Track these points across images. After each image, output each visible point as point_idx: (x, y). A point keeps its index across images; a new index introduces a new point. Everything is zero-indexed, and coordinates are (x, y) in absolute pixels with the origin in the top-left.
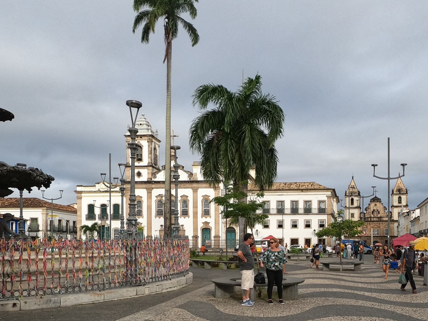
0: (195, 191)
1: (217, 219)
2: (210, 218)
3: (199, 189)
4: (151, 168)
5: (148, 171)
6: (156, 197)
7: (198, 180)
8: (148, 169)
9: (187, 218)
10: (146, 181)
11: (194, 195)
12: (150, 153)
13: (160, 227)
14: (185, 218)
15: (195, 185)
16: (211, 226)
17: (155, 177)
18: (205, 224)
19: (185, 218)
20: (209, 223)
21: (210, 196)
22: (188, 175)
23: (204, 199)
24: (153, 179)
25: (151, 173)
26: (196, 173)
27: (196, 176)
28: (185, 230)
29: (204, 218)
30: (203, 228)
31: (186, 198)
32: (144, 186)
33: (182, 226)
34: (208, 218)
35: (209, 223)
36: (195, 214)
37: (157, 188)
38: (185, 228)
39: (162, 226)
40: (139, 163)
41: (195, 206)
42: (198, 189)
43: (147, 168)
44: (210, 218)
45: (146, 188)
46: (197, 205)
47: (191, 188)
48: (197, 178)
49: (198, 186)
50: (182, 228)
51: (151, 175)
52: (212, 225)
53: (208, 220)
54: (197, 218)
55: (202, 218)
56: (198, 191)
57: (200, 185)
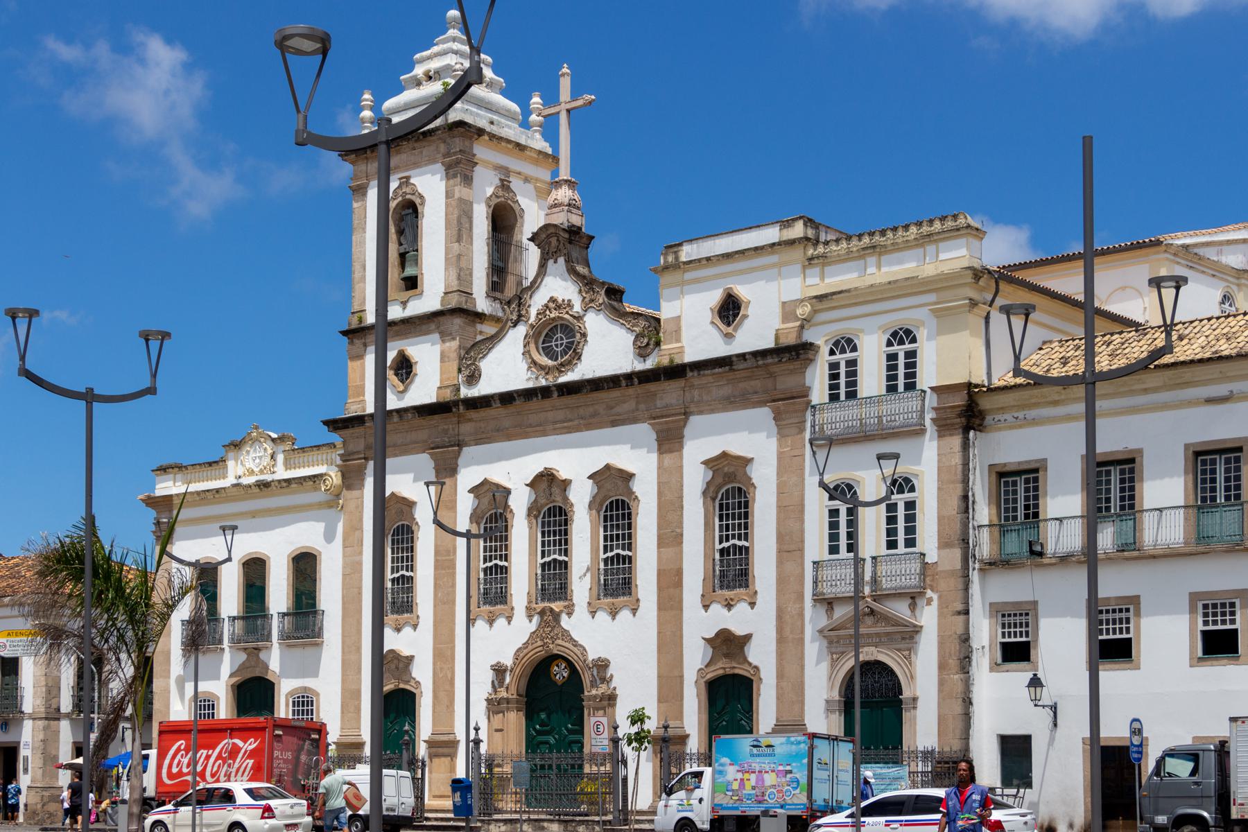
1: (792, 608)
2: (752, 605)
4: (458, 321)
7: (689, 358)
9: (625, 614)
10: (434, 400)
12: (455, 233)
14: (614, 618)
17: (473, 378)
19: (614, 619)
24: (466, 392)
25: (454, 355)
26: (679, 317)
27: (678, 340)
29: (716, 608)
30: (709, 676)
32: (423, 435)
33: (602, 665)
34: (742, 607)
35: (748, 637)
36: (670, 581)
40: (404, 304)
41: (670, 537)
42: (685, 421)
45: (432, 447)
48: (681, 351)
53: (720, 618)
54: (680, 608)
55: (706, 607)
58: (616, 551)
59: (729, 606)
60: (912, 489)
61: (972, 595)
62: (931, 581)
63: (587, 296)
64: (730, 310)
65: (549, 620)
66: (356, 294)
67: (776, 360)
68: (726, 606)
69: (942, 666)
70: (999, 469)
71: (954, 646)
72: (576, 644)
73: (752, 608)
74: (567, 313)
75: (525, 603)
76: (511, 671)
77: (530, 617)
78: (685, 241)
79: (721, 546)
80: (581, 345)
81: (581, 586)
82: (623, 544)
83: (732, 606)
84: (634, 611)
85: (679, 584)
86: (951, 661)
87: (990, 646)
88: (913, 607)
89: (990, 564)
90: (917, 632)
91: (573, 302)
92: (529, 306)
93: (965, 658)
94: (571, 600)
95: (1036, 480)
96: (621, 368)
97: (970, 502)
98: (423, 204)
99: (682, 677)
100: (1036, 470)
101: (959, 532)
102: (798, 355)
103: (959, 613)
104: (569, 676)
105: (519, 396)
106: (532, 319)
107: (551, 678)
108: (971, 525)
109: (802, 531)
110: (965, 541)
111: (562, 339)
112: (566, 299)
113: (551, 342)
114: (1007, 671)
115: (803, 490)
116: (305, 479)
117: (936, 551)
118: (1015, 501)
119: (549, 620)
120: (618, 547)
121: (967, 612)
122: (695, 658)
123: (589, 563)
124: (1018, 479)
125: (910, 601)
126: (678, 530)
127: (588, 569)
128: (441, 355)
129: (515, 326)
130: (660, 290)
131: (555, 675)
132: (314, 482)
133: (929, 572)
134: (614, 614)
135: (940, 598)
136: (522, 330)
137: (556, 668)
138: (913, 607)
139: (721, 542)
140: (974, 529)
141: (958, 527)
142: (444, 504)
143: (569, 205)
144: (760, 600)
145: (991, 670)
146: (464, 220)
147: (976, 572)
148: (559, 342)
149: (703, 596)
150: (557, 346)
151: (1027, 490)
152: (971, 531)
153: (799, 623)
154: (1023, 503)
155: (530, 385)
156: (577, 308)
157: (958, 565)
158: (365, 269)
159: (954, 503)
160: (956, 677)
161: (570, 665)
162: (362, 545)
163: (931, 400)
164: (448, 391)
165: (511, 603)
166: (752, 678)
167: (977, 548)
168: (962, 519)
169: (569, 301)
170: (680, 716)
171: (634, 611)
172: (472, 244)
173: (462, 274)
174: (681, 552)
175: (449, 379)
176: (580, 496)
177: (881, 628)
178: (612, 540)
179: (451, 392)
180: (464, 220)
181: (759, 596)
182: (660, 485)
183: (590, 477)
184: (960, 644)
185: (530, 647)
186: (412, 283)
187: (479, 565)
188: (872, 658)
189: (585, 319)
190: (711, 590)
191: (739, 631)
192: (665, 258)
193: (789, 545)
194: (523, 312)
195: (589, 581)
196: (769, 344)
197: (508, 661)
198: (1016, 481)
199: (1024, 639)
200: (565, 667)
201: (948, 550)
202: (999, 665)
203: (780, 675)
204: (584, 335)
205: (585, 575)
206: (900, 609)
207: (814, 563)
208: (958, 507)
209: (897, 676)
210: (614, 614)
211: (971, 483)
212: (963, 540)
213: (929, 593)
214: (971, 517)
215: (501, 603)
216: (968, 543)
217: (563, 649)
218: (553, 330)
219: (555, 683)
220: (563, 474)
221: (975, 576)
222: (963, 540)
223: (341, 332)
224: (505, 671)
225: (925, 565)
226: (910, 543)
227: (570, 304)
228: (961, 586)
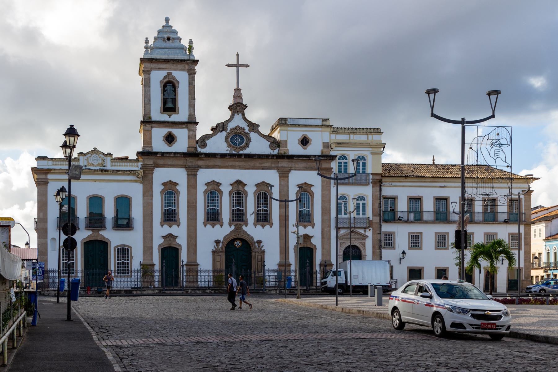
0: (284, 175)
1: (326, 229)
2: (313, 227)
3: (292, 171)
5: (189, 132)
6: (207, 184)
7: (291, 153)
8: (189, 130)
9: (267, 227)
11: (282, 183)
13: (215, 244)
14: (263, 228)
15: (284, 164)
16: (314, 244)
17: (204, 146)
19: (263, 228)
20: (312, 237)
21: (312, 185)
24: (200, 150)
28: (264, 252)
31: (266, 189)
32: (181, 162)
33: (259, 242)
34: (309, 228)
35: (312, 237)
36: (284, 219)
37: (207, 167)
38: (266, 247)
39: (217, 242)
43: (187, 127)
44: (313, 227)
47: (274, 169)
48: (288, 150)
49: (290, 166)
50: (259, 246)
51: (195, 142)
52: (317, 242)
56: (290, 175)
57: (293, 164)
58: (262, 208)
59: (305, 227)
60: (364, 200)
63: (251, 127)
64: (305, 142)
65: (238, 229)
67: (325, 159)
72: (248, 235)
73: (313, 228)
74: (243, 132)
75: (228, 221)
76: (222, 243)
79: (300, 210)
80: (248, 142)
81: (251, 218)
91: (245, 128)
94: (247, 221)
96: (264, 152)
102: (333, 158)
104: (242, 245)
106: (228, 131)
111: (238, 139)
112: (242, 127)
115: (330, 196)
116: (127, 171)
119: (238, 229)
120: (263, 207)
122: (293, 241)
125: (364, 230)
127: (253, 213)
129: (221, 132)
132: (131, 172)
134: (263, 227)
136: (224, 134)
139: (300, 208)
153: (329, 234)
155: (228, 152)
156: (247, 130)
157: (379, 221)
161: (242, 240)
162: (152, 196)
164: (193, 149)
176: (251, 190)
177: (356, 236)
178: (260, 204)
179: (194, 150)
182: (280, 189)
183: (256, 185)
188: (354, 244)
191: (310, 235)
192: (281, 122)
193: (326, 211)
194: (225, 128)
196: (319, 153)
197: (222, 240)
205: (252, 214)
210: (263, 227)
218: (235, 136)
219: (236, 247)
227: (244, 129)
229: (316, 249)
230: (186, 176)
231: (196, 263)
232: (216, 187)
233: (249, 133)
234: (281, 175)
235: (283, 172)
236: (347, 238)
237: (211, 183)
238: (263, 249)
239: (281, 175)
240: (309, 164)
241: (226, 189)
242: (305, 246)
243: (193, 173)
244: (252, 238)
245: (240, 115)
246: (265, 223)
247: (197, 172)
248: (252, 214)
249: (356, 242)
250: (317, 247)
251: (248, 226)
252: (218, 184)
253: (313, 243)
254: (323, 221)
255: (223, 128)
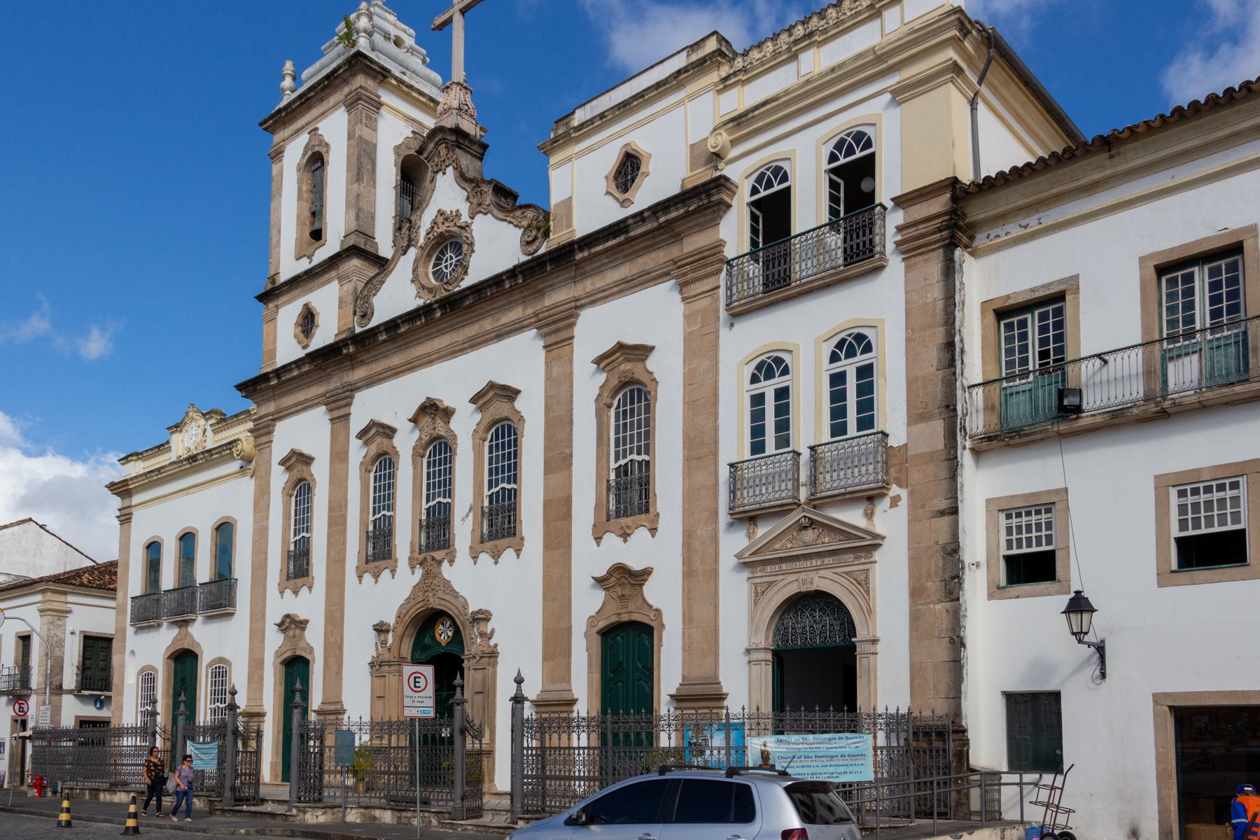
1: (702, 532)
2: (653, 531)
11: (555, 372)
12: (355, 172)
16: (655, 606)
17: (366, 316)
18: (618, 589)
20: (646, 573)
22: (519, 232)
23: (615, 382)
26: (570, 199)
29: (611, 539)
30: (602, 625)
33: (482, 617)
34: (641, 534)
35: (646, 573)
39: (381, 629)
40: (310, 257)
46: (571, 446)
51: (352, 312)
54: (569, 546)
55: (598, 539)
59: (625, 536)
61: (962, 485)
62: (897, 472)
66: (273, 260)
68: (621, 536)
69: (916, 593)
70: (997, 305)
71: (936, 562)
72: (456, 595)
77: (413, 568)
78: (578, 107)
81: (463, 530)
82: (509, 477)
83: (629, 535)
84: (518, 551)
85: (567, 516)
86: (929, 584)
87: (988, 561)
88: (869, 515)
89: (990, 439)
90: (877, 546)
91: (461, 212)
92: (419, 227)
93: (953, 578)
95: (1059, 312)
97: (958, 350)
98: (328, 152)
99: (569, 629)
100: (1060, 297)
101: (940, 396)
103: (942, 513)
104: (454, 634)
105: (403, 322)
107: (435, 638)
108: (958, 383)
109: (716, 429)
110: (950, 407)
113: (441, 264)
114: (1018, 597)
117: (905, 428)
118: (1024, 349)
121: (954, 511)
123: (471, 502)
124: (1029, 316)
126: (567, 451)
127: (471, 509)
128: (340, 301)
130: (549, 172)
131: (441, 635)
133: (894, 461)
134: (496, 556)
135: (911, 494)
137: (441, 627)
138: (869, 515)
140: (963, 388)
141: (938, 390)
142: (339, 455)
143: (460, 109)
144: (661, 525)
145: (991, 596)
146: (365, 160)
147: (967, 454)
148: (449, 262)
149: (594, 525)
150: (446, 267)
151: (1043, 329)
152: (959, 393)
153: (712, 550)
154: (1037, 349)
156: (465, 218)
158: (280, 233)
159: (932, 355)
160: (939, 607)
163: (896, 218)
165: (395, 555)
166: (653, 624)
167: (968, 418)
168: (945, 377)
169: (458, 211)
170: (567, 678)
171: (518, 551)
172: (374, 186)
173: (361, 215)
174: (570, 476)
175: (345, 324)
180: (365, 160)
181: (661, 520)
182: (548, 398)
184: (944, 558)
185: (413, 602)
186: (317, 235)
187: (368, 518)
189: (473, 227)
190: (604, 519)
191: (636, 566)
195: (471, 523)
197: (391, 620)
198: (1026, 320)
199: (1044, 548)
200: (450, 626)
201: (924, 424)
202: (1004, 588)
203: (688, 619)
204: (471, 244)
205: (467, 516)
206: (853, 516)
207: (731, 465)
208: (939, 360)
209: (848, 613)
211: (957, 324)
212: (947, 406)
213: (894, 490)
214: (958, 371)
215: (384, 558)
216: (955, 410)
217: (444, 603)
220: (447, 402)
221: (966, 458)
222: (947, 406)
223: (257, 298)
224: (387, 631)
225: (888, 450)
226: (866, 423)
227: (458, 215)
228: (943, 473)
229: (663, 626)
230: (328, 425)
231: (338, 707)
232: (386, 441)
233: (470, 221)
234: (552, 339)
235: (553, 327)
236: (782, 560)
237: (373, 431)
238: (492, 643)
239: (552, 339)
240: (641, 260)
241: (406, 441)
242: (625, 618)
243: (342, 412)
244: (465, 605)
245: (450, 170)
246: (501, 543)
247: (349, 404)
248: (467, 516)
249: (822, 573)
250: (665, 620)
251: (456, 559)
252: (387, 431)
253: (651, 602)
254: (690, 497)
255: (409, 235)
